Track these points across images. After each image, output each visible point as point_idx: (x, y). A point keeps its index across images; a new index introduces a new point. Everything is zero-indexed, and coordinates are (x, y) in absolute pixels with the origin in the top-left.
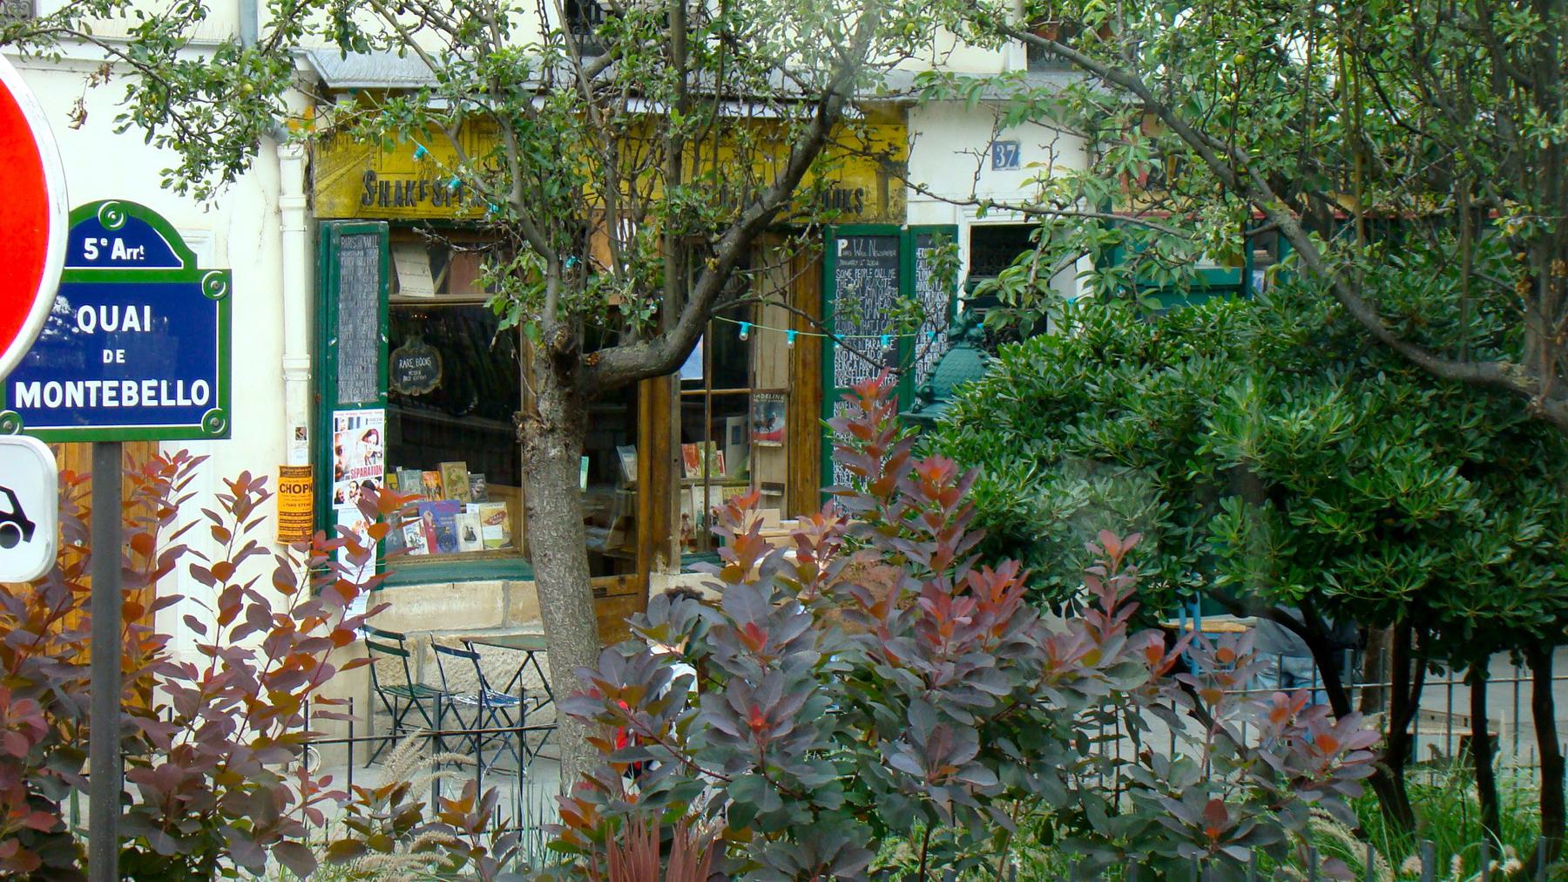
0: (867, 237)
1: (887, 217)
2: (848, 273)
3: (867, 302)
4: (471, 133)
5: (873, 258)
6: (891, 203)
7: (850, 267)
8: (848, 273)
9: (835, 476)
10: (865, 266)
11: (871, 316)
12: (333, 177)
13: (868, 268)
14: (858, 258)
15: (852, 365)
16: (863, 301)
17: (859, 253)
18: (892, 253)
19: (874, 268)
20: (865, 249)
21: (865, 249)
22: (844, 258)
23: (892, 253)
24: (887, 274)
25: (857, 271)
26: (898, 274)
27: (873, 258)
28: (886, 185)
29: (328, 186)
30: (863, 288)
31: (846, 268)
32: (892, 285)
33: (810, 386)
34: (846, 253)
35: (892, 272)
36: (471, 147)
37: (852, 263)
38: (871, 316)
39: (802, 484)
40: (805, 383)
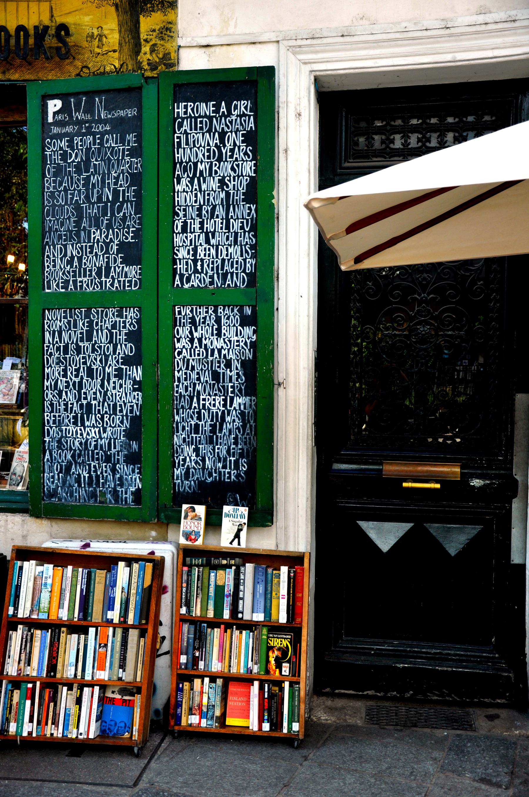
0: (91, 94)
1: (139, 66)
2: (64, 144)
3: (93, 180)
5: (100, 121)
6: (146, 48)
7: (66, 134)
8: (64, 144)
9: (47, 404)
11: (100, 199)
13: (94, 134)
14: (79, 123)
15: (70, 262)
16: (87, 180)
17: (80, 116)
18: (131, 113)
19: (103, 134)
20: (90, 109)
21: (90, 109)
22: (56, 123)
23: (131, 113)
24: (123, 141)
25: (77, 140)
26: (139, 139)
27: (100, 121)
28: (138, 22)
30: (87, 162)
31: (60, 136)
32: (131, 155)
34: (60, 117)
35: (131, 137)
37: (69, 129)
38: (100, 199)
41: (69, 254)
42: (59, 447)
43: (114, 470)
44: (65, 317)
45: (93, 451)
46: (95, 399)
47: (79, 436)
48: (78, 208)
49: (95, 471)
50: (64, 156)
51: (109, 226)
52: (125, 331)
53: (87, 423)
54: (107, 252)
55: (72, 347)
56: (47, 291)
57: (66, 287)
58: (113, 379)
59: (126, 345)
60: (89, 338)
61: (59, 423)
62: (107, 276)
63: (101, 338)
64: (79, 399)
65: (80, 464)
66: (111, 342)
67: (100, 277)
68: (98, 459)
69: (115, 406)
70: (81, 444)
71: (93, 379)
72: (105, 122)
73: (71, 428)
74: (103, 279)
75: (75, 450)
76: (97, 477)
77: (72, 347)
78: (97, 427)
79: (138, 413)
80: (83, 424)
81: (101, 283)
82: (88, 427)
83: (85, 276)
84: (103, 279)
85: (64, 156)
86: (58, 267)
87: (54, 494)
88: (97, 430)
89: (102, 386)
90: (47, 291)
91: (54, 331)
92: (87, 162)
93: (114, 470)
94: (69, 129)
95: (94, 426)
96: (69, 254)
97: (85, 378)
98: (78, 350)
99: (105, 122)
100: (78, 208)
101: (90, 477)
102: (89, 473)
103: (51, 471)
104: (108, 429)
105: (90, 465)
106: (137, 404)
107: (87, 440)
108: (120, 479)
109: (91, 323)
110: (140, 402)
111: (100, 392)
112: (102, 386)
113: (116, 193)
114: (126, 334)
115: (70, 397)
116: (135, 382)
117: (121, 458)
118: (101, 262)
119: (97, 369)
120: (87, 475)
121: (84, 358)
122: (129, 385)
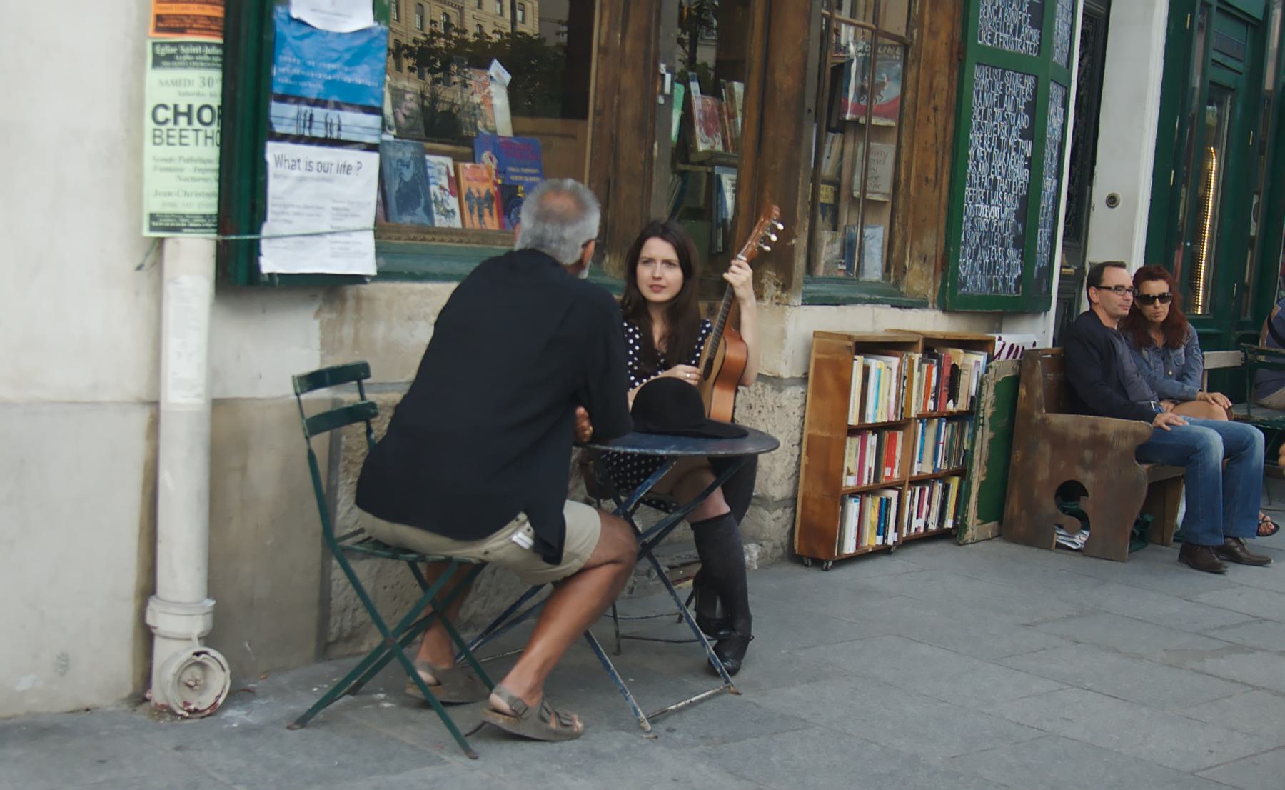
15: (997, 13)
33: (943, 36)
39: (919, 186)
41: (997, 4)
42: (972, 228)
43: (1005, 255)
44: (988, 77)
45: (994, 233)
46: (1000, 174)
47: (986, 216)
49: (994, 257)
52: (1024, 101)
53: (992, 202)
54: (1021, 10)
56: (979, 42)
57: (991, 41)
58: (1013, 153)
59: (1023, 116)
60: (1001, 106)
62: (1019, 37)
63: (1009, 106)
64: (989, 175)
65: (984, 248)
66: (1014, 111)
67: (1014, 37)
68: (996, 244)
69: (1012, 182)
70: (986, 225)
71: (1000, 151)
73: (982, 206)
74: (1016, 39)
75: (982, 232)
76: (995, 262)
77: (990, 111)
78: (999, 206)
79: (1025, 193)
80: (989, 203)
81: (1014, 42)
82: (993, 205)
83: (1005, 32)
84: (1016, 39)
86: (988, 15)
88: (998, 209)
89: (1006, 160)
90: (979, 42)
91: (979, 91)
93: (1005, 255)
95: (997, 206)
96: (997, 4)
97: (995, 149)
101: (990, 263)
102: (989, 259)
103: (964, 257)
104: (1006, 208)
105: (990, 249)
106: (1025, 182)
107: (991, 220)
108: (1009, 264)
109: (1004, 85)
110: (1027, 181)
111: (1004, 166)
112: (1006, 160)
114: (1025, 104)
115: (983, 169)
116: (1027, 159)
117: (1011, 241)
118: (1016, 20)
119: (1004, 140)
120: (988, 261)
121: (996, 126)
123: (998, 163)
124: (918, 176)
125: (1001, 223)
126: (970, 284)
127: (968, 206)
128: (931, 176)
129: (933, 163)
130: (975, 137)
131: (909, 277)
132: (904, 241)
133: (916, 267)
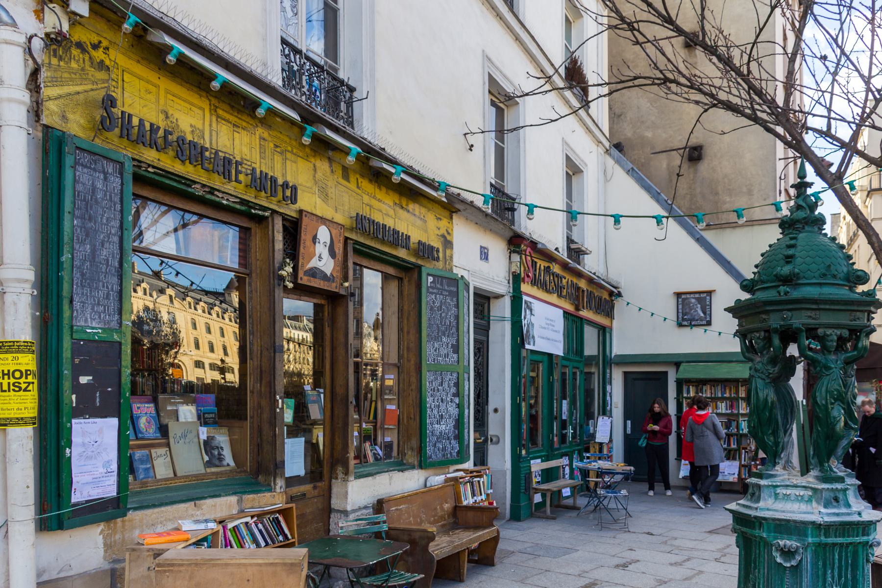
3: (443, 315)
4: (211, 115)
5: (445, 290)
10: (441, 294)
12: (66, 90)
13: (443, 295)
15: (436, 350)
16: (441, 314)
17: (439, 286)
19: (446, 296)
20: (442, 284)
25: (438, 296)
27: (445, 290)
29: (60, 97)
33: (413, 362)
34: (432, 285)
35: (455, 299)
36: (211, 125)
37: (435, 291)
39: (408, 421)
40: (409, 361)
48: (438, 327)
50: (434, 302)
51: (448, 336)
55: (436, 389)
60: (442, 386)
61: (432, 424)
63: (446, 385)
72: (447, 291)
73: (436, 426)
77: (436, 389)
85: (434, 302)
87: (430, 457)
92: (441, 306)
94: (435, 291)
98: (438, 390)
99: (447, 291)
100: (438, 327)
113: (450, 322)
115: (435, 412)
118: (446, 352)
122: (454, 405)
123: (443, 407)
124: (407, 417)
125: (447, 431)
126: (433, 457)
127: (429, 427)
128: (412, 416)
129: (412, 411)
130: (429, 400)
131: (407, 457)
132: (404, 443)
133: (410, 453)
